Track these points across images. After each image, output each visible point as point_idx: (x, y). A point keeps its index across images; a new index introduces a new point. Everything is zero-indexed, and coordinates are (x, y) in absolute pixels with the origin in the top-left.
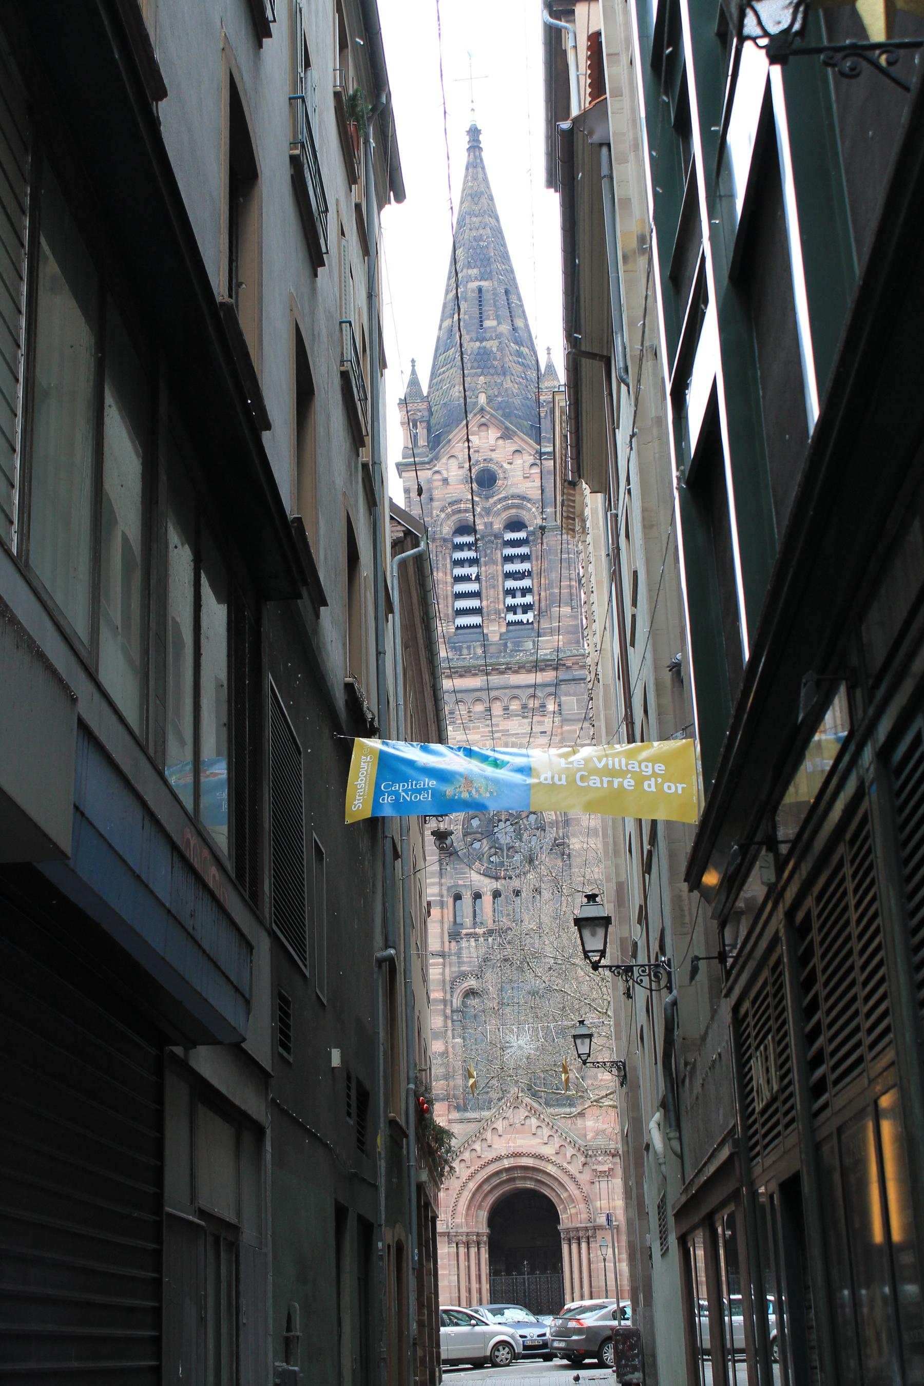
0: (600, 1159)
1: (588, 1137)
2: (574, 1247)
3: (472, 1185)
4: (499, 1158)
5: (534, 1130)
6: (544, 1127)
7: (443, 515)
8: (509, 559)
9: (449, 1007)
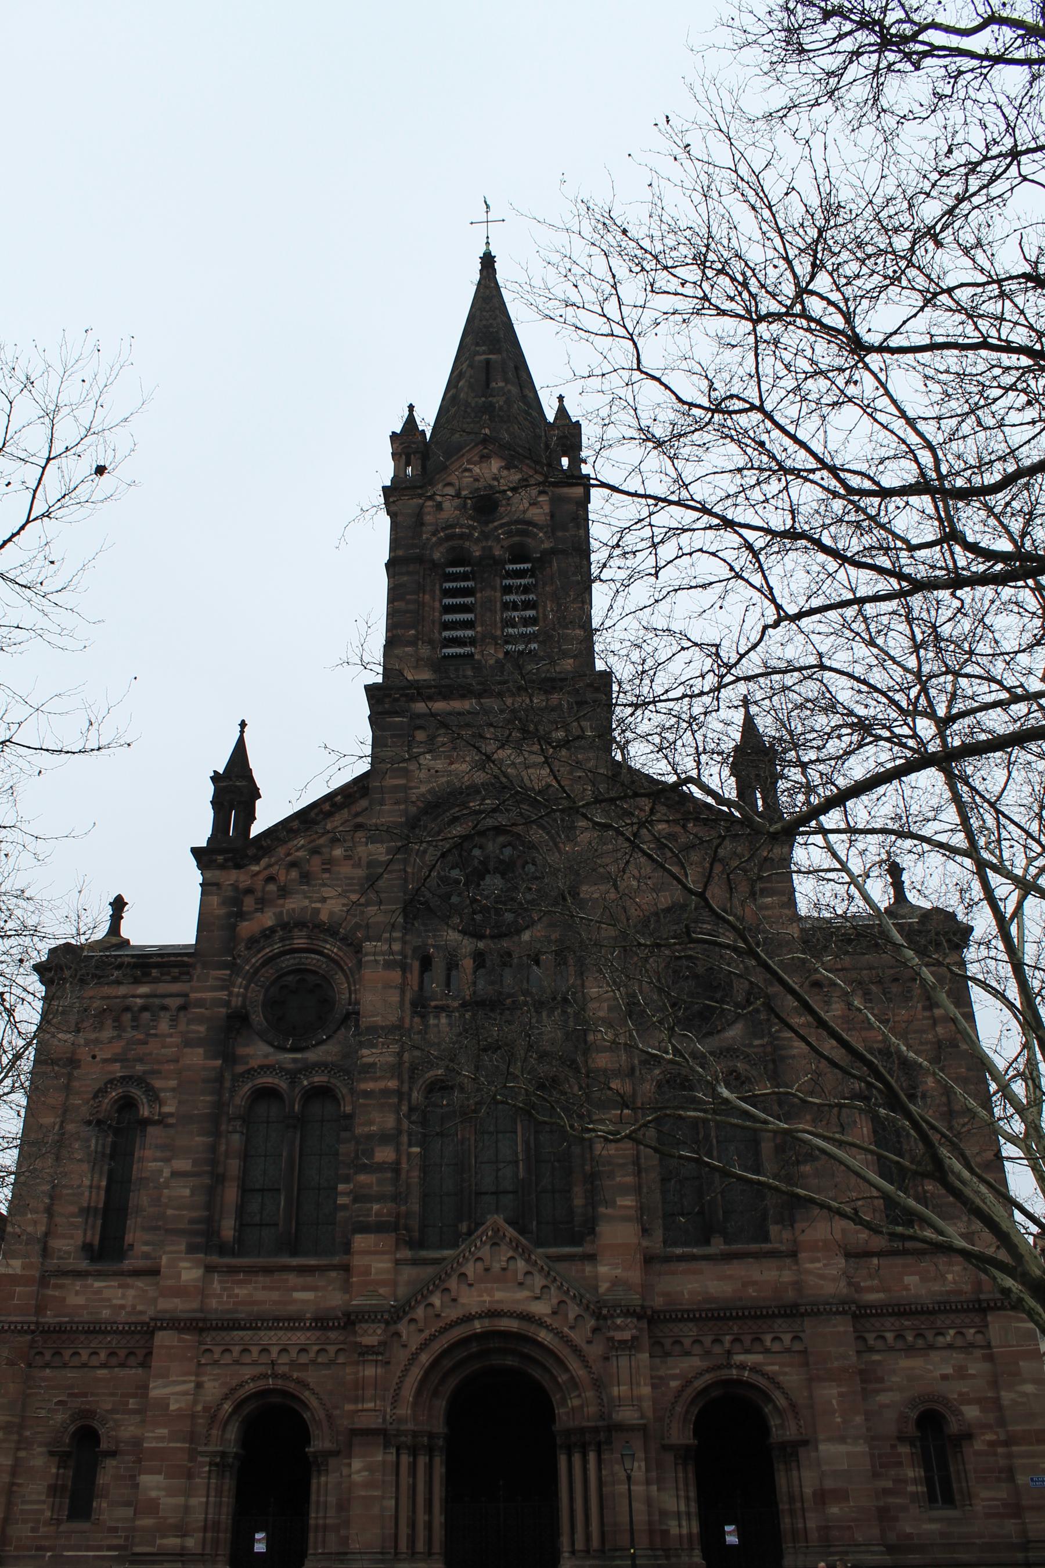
0: (619, 1321)
1: (601, 1290)
2: (577, 1458)
3: (425, 1358)
4: (468, 1318)
5: (520, 1277)
6: (536, 1274)
7: (434, 539)
8: (508, 590)
9: (405, 1103)
